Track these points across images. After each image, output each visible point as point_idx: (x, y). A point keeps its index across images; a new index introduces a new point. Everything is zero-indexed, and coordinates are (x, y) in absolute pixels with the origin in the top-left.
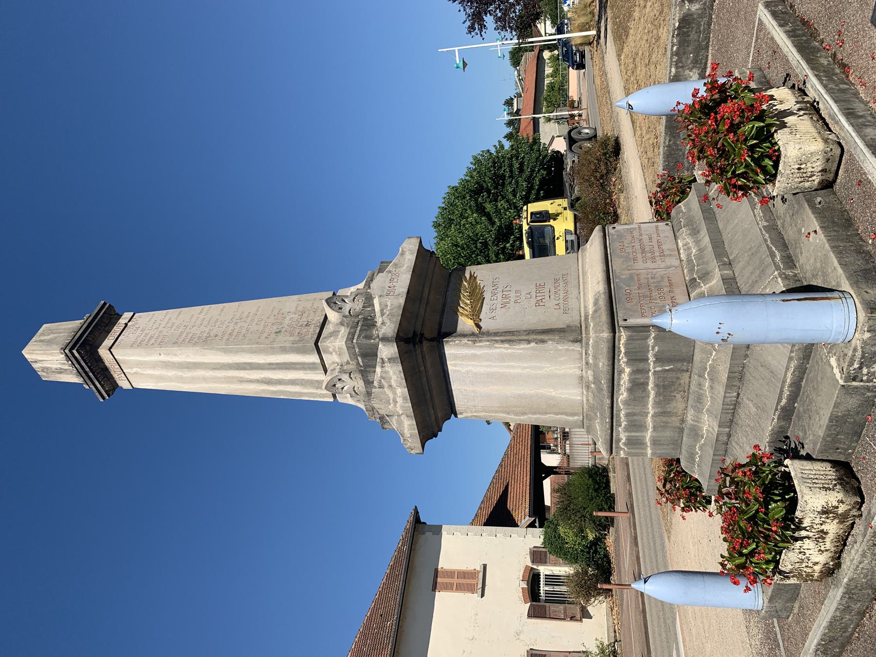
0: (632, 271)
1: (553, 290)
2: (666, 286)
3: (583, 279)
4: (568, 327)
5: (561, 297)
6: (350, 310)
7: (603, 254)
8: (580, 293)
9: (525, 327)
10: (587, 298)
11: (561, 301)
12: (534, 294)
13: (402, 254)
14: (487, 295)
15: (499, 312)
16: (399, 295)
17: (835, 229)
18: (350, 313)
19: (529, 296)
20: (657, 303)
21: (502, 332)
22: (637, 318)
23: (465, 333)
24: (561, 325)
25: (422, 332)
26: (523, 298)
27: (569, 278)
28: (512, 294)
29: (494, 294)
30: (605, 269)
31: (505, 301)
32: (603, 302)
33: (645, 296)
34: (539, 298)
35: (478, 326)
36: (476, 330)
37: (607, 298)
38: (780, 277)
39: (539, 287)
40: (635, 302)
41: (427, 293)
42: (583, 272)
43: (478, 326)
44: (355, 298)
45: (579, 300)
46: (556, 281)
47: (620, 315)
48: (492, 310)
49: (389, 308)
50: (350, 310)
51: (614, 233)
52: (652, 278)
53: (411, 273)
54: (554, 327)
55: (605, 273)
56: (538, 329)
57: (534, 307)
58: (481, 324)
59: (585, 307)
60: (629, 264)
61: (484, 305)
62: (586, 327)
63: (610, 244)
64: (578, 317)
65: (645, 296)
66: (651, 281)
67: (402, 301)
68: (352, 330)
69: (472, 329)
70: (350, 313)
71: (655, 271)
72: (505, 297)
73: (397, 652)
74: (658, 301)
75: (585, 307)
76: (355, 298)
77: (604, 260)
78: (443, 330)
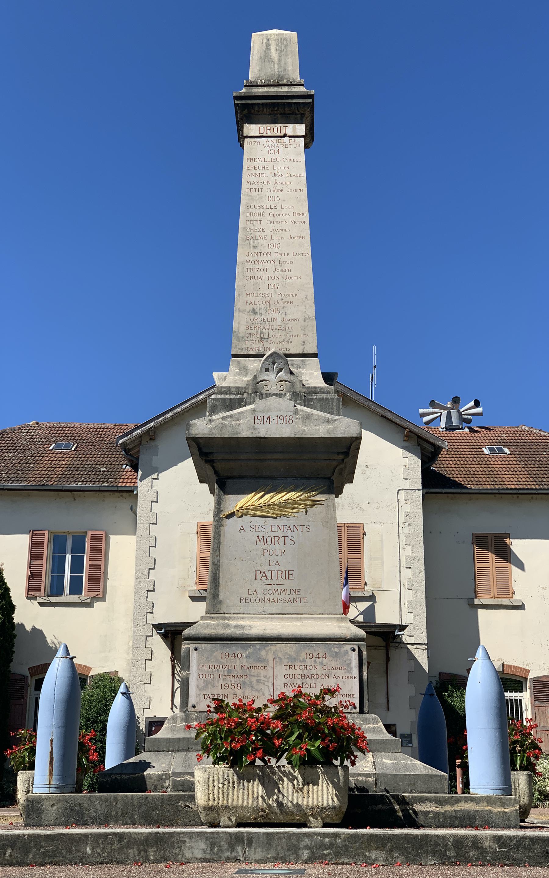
0: (271, 662)
1: (279, 588)
2: (244, 693)
3: (289, 618)
4: (220, 602)
5: (268, 596)
6: (266, 381)
7: (309, 636)
8: (271, 614)
9: (224, 561)
10: (254, 620)
11: (260, 596)
12: (277, 568)
13: (328, 421)
14: (280, 521)
15: (252, 535)
16: (255, 429)
17: (143, 808)
18: (262, 381)
19: (274, 564)
20: (218, 681)
21: (219, 539)
22: (198, 660)
23: (222, 504)
24: (222, 595)
25: (215, 461)
26: (272, 558)
27: (299, 604)
28: (277, 547)
29: (281, 528)
30: (283, 636)
31: (269, 540)
32: (238, 632)
33: (229, 671)
34: (269, 574)
35: (232, 515)
36: (226, 513)
37: (235, 636)
38: (163, 774)
39: (288, 575)
40: (222, 661)
41: (274, 458)
42: (301, 618)
43: (232, 515)
44: (286, 381)
45: (261, 613)
46: (297, 591)
47: (203, 646)
48: (256, 528)
49: (234, 422)
50: (266, 381)
51: (342, 649)
52: (258, 681)
53: (293, 436)
54: (221, 589)
55: (275, 636)
56: (221, 574)
57: (255, 569)
58: (235, 518)
59: (243, 618)
60: (285, 661)
61: (264, 519)
62: (212, 618)
63: (327, 644)
64: (233, 612)
65: (229, 671)
66: (254, 679)
67: (245, 433)
68: (233, 390)
69: (227, 510)
70: (262, 381)
71: (270, 685)
72: (274, 540)
73: (532, 498)
74: (221, 682)
75: (243, 618)
76: (286, 381)
77: (299, 636)
78: (229, 482)
